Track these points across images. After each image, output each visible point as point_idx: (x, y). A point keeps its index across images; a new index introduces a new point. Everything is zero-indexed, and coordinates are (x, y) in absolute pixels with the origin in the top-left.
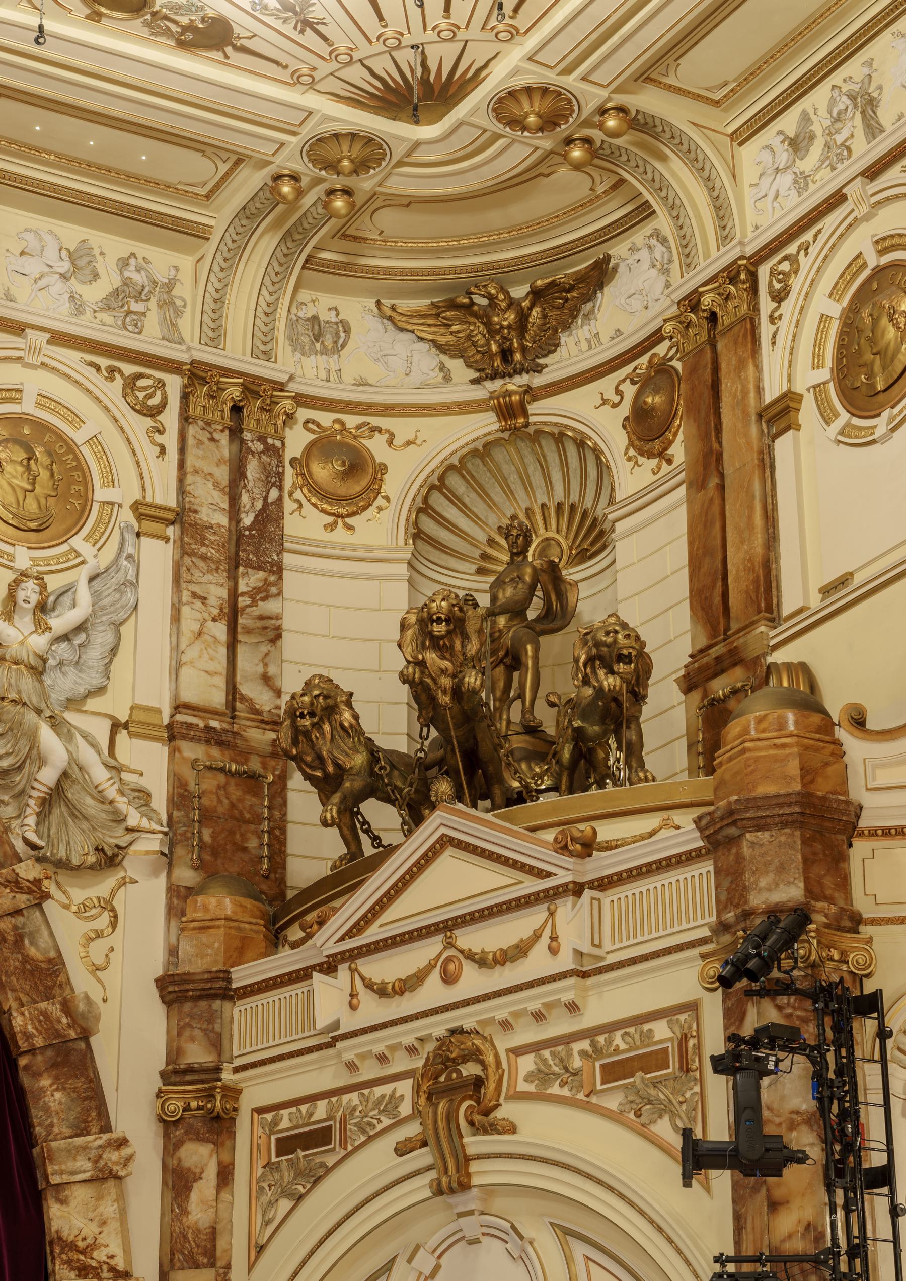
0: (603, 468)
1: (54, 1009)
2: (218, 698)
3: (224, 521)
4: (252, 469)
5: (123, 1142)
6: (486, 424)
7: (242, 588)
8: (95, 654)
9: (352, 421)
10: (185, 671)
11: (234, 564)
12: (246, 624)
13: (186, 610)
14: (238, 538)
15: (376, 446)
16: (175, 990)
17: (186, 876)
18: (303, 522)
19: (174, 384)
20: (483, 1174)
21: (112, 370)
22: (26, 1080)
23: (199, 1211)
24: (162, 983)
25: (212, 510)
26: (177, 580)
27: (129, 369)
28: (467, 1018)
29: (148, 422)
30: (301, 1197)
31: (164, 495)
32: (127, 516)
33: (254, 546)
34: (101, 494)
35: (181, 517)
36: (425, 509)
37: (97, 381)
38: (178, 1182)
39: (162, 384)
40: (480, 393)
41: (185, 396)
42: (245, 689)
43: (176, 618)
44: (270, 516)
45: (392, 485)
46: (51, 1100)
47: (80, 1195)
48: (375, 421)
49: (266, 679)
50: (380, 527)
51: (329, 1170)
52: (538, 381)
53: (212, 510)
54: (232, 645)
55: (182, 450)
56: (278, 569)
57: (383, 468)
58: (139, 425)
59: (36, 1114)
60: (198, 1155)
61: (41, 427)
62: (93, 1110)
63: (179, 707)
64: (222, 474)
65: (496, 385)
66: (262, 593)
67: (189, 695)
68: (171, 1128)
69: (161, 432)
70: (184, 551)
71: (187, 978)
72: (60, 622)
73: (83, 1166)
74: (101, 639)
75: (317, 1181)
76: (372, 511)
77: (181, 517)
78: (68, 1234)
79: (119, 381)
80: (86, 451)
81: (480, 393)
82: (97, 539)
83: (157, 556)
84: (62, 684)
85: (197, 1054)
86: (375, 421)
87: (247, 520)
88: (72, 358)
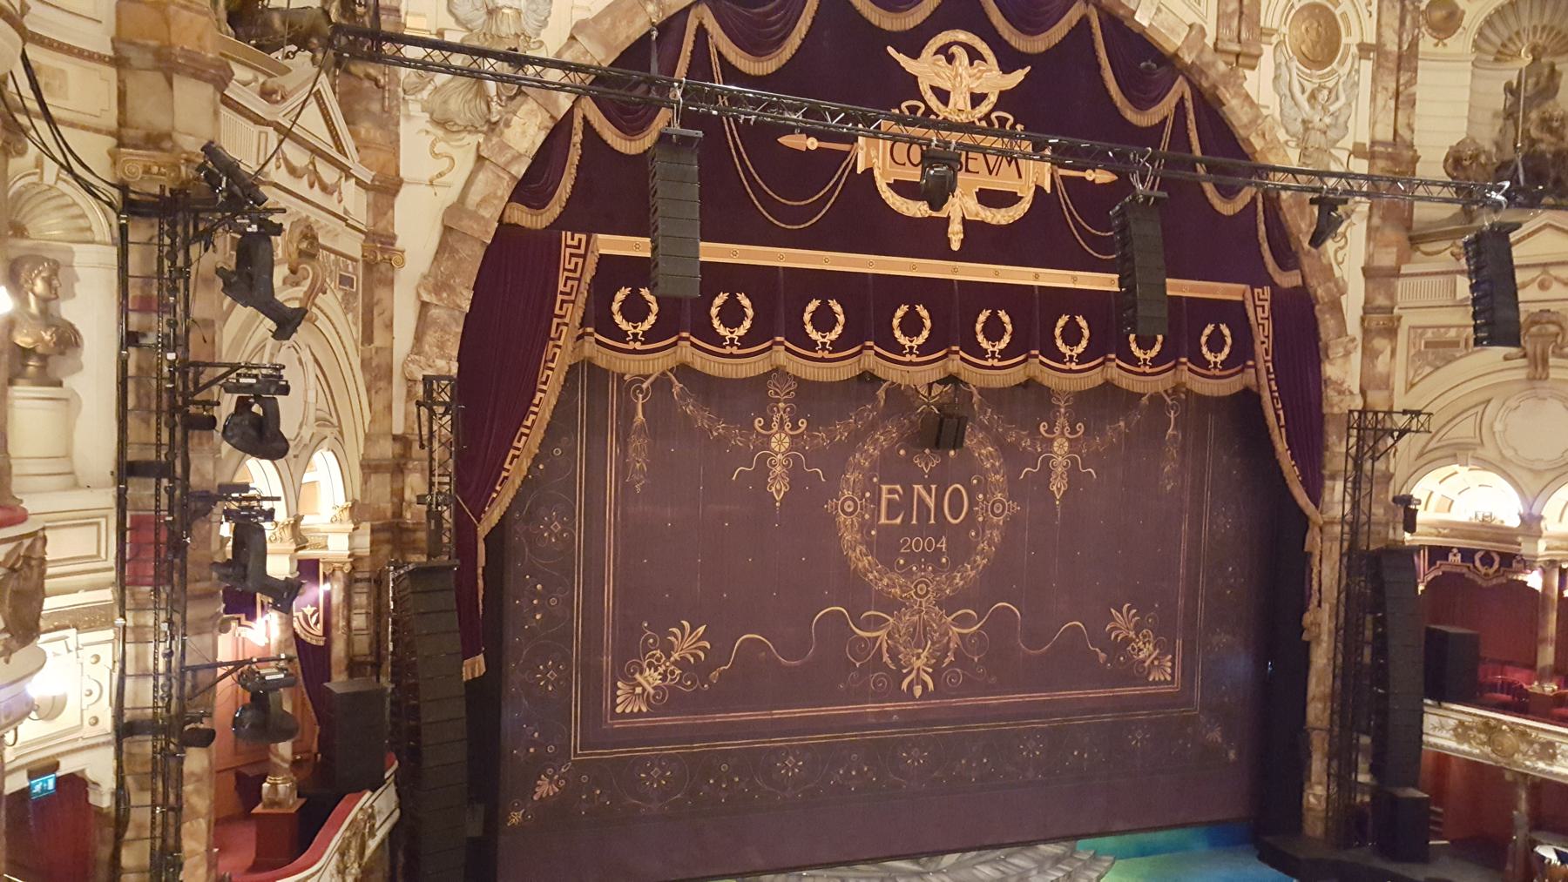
1: (1332, 285)
2: (1390, 137)
3: (1396, 48)
4: (1408, 22)
5: (1353, 340)
7: (1402, 81)
8: (1342, 120)
10: (1379, 127)
11: (1399, 69)
12: (1403, 100)
13: (1379, 96)
14: (1400, 57)
16: (1368, 272)
17: (1376, 221)
18: (1427, 44)
20: (1553, 374)
22: (1318, 314)
23: (1382, 364)
24: (1365, 271)
25: (1392, 47)
26: (1374, 80)
28: (1553, 307)
30: (1438, 368)
31: (1371, 39)
32: (1354, 50)
33: (1407, 60)
34: (1344, 40)
35: (1378, 48)
36: (1480, 33)
38: (1369, 354)
42: (1401, 131)
43: (1373, 98)
44: (1414, 44)
45: (1465, 23)
46: (1327, 325)
47: (1339, 362)
49: (1410, 127)
50: (1461, 43)
51: (1457, 359)
53: (1392, 47)
54: (1397, 108)
55: (1379, 14)
56: (1415, 70)
57: (1463, 12)
59: (1322, 329)
60: (1380, 343)
62: (1342, 322)
63: (1373, 143)
64: (1396, 24)
66: (1412, 82)
67: (1379, 137)
68: (1366, 332)
70: (1378, 66)
71: (1375, 269)
72: (1332, 109)
73: (1341, 351)
74: (1345, 112)
75: (1449, 362)
77: (1378, 48)
78: (1334, 378)
82: (1342, 63)
83: (1367, 67)
84: (1332, 134)
85: (1381, 301)
87: (1405, 47)
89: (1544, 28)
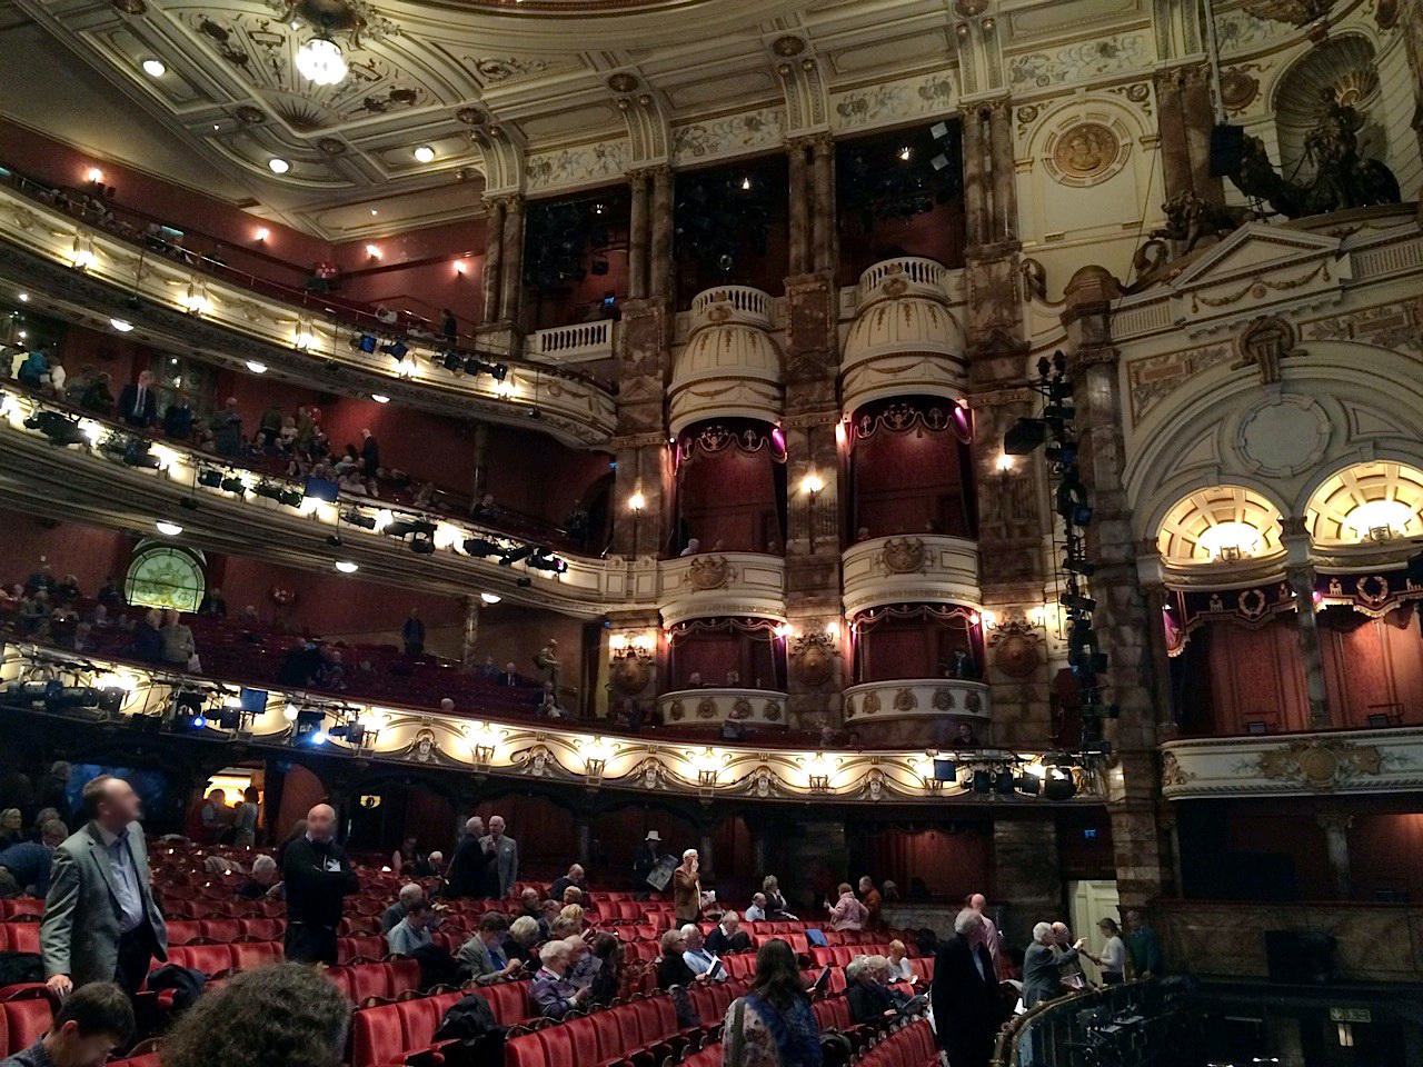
0: (1370, 46)
6: (1309, 45)
9: (1238, 66)
15: (1253, 74)
19: (1150, 83)
21: (1120, 90)
27: (1128, 86)
29: (1142, 103)
37: (1113, 97)
39: (1146, 85)
40: (1302, 32)
41: (1155, 86)
45: (1262, 89)
48: (1250, 63)
52: (1330, 17)
57: (1258, 81)
58: (1136, 107)
61: (1089, 126)
65: (1308, 27)
69: (1148, 104)
76: (1254, 102)
79: (1124, 92)
80: (1113, 129)
81: (1302, 32)
86: (1250, 63)
88: (1102, 93)
89: (1361, 73)
